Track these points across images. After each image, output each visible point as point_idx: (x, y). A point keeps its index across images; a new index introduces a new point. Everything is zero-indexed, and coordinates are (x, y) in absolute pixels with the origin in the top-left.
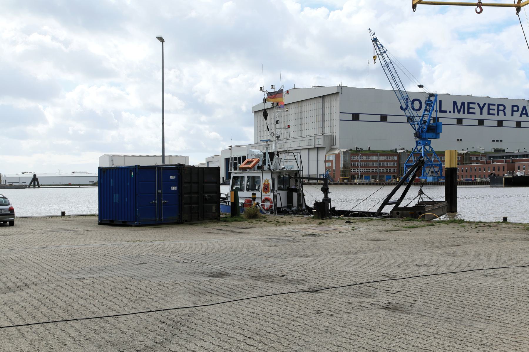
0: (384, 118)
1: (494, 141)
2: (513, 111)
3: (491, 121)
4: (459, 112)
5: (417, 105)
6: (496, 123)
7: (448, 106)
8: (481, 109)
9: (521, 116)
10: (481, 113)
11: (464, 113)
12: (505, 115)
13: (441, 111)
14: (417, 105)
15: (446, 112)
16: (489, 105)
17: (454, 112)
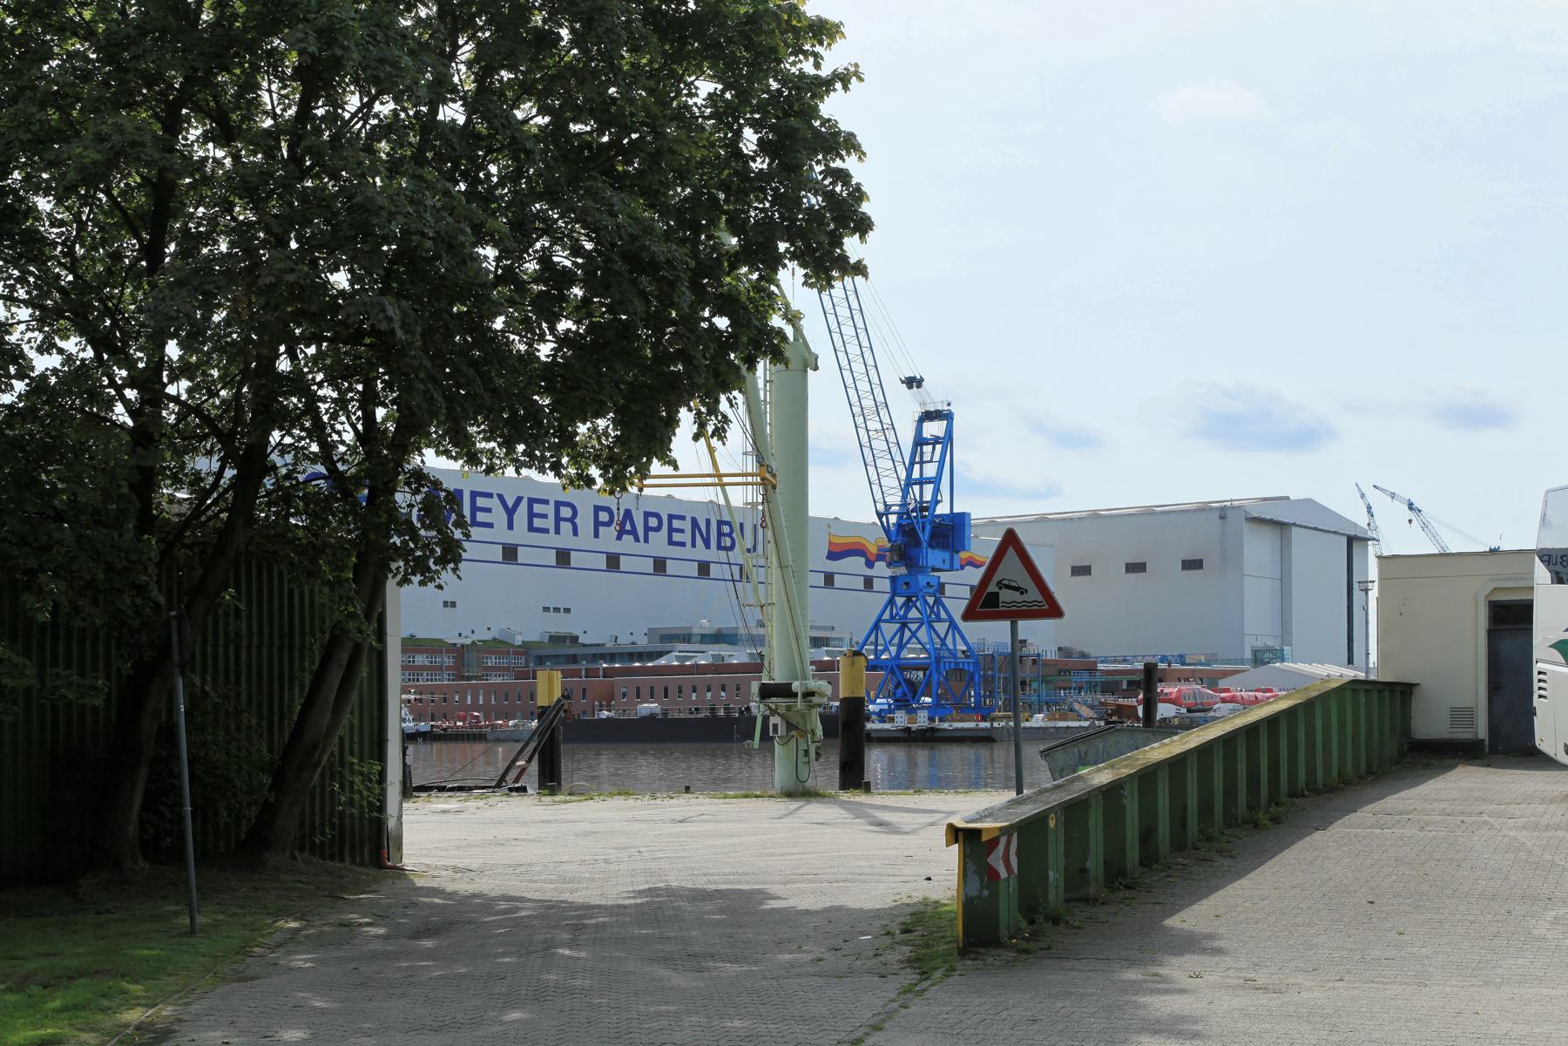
1: (546, 609)
2: (598, 524)
3: (537, 550)
8: (511, 512)
9: (619, 538)
10: (510, 526)
12: (575, 533)
16: (532, 501)
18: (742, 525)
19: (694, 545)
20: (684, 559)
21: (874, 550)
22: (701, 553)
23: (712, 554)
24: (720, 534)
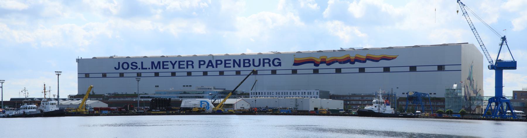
0: (104, 75)
1: (184, 86)
2: (200, 65)
4: (156, 68)
5: (125, 66)
6: (186, 74)
7: (147, 65)
8: (173, 65)
9: (207, 67)
10: (173, 68)
11: (160, 68)
12: (193, 67)
13: (142, 68)
14: (125, 66)
15: (146, 69)
16: (179, 62)
17: (152, 68)
18: (253, 60)
19: (234, 66)
20: (232, 70)
21: (319, 60)
22: (237, 68)
23: (242, 68)
24: (244, 63)
